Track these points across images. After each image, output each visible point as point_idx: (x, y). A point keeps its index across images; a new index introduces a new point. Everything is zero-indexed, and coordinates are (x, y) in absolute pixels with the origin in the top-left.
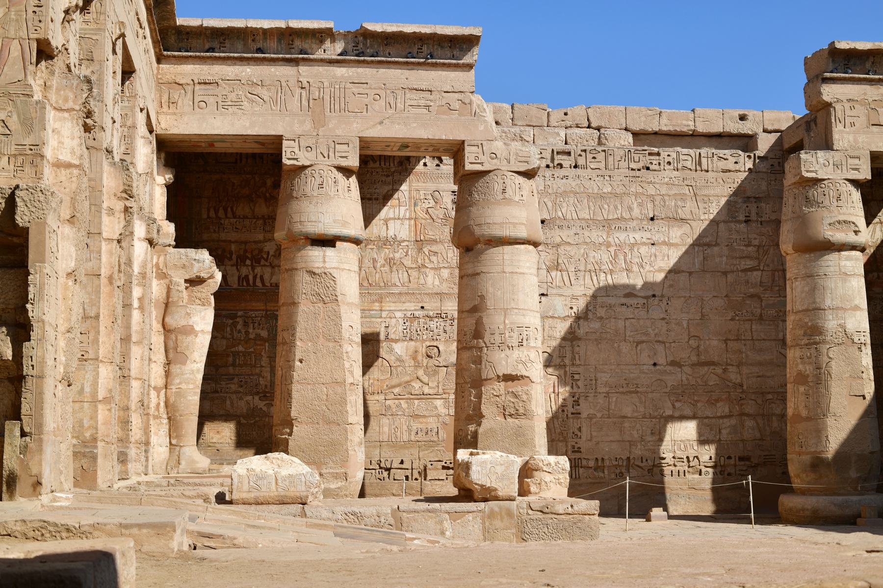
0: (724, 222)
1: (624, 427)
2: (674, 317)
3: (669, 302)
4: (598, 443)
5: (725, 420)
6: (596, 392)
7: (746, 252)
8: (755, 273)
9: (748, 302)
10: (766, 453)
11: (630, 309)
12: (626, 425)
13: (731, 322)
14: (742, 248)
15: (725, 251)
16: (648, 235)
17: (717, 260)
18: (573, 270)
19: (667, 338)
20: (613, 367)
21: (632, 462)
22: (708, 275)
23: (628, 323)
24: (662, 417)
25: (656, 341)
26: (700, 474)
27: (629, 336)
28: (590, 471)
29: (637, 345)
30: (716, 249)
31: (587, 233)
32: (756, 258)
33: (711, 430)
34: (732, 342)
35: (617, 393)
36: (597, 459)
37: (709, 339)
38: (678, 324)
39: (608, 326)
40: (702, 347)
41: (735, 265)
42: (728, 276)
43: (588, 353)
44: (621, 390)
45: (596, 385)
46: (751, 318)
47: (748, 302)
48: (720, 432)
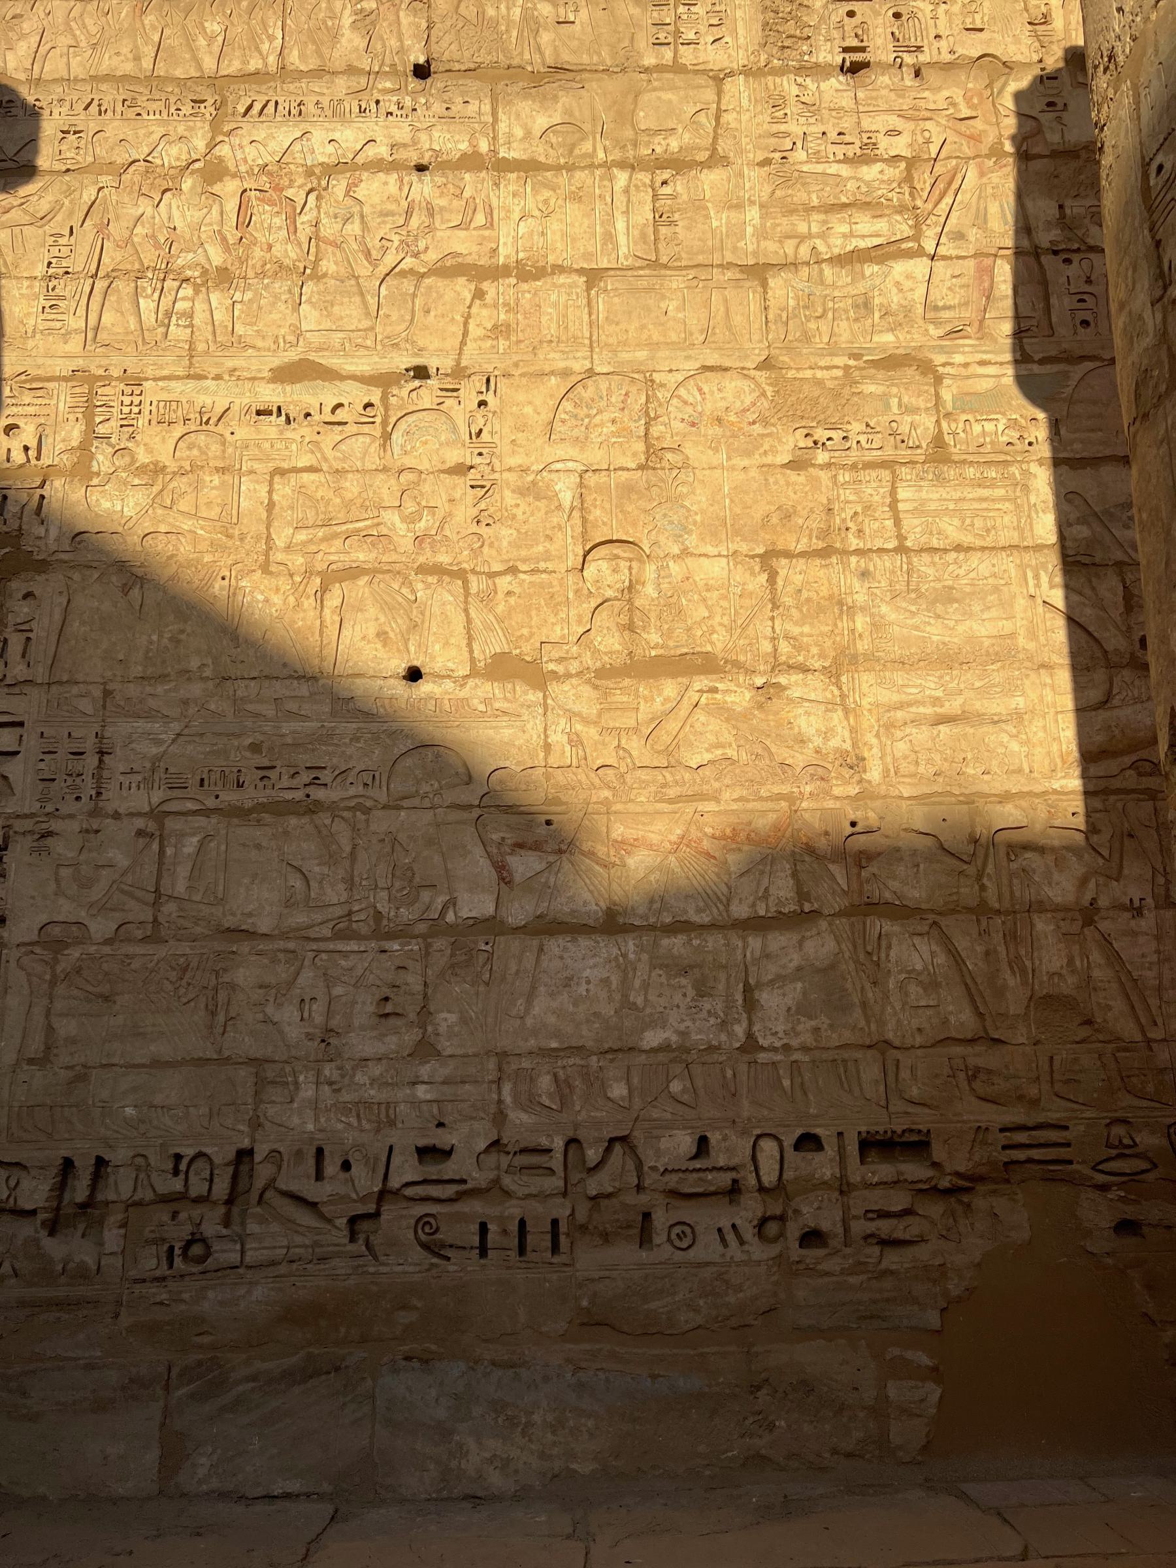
0: (747, 72)
1: (233, 987)
2: (513, 461)
3: (489, 397)
4: (81, 1077)
5: (778, 941)
6: (95, 813)
7: (851, 185)
8: (899, 268)
9: (870, 388)
10: (1016, 1115)
11: (302, 431)
12: (244, 976)
13: (793, 476)
14: (833, 169)
15: (755, 182)
16: (402, 132)
17: (719, 220)
18: (40, 270)
19: (476, 553)
20: (196, 689)
21: (264, 1172)
22: (676, 282)
23: (284, 490)
24: (437, 927)
25: (423, 570)
26: (645, 1237)
27: (288, 548)
28: (26, 1229)
29: (324, 589)
30: (711, 179)
31: (114, 129)
32: (901, 209)
33: (703, 991)
34: (801, 563)
35: (206, 812)
36: (68, 1164)
37: (685, 553)
38: (531, 491)
39: (184, 505)
40: (650, 590)
41: (802, 239)
42: (772, 283)
43: (75, 626)
44: (230, 797)
45: (98, 777)
46: (889, 453)
47: (870, 388)
48: (750, 1004)
